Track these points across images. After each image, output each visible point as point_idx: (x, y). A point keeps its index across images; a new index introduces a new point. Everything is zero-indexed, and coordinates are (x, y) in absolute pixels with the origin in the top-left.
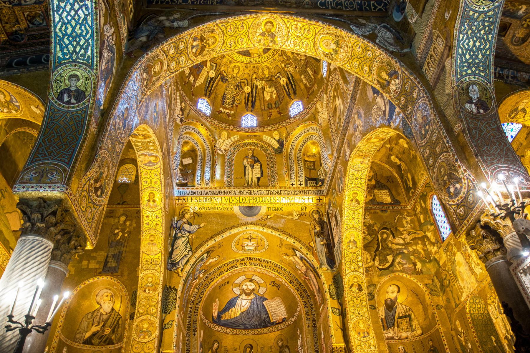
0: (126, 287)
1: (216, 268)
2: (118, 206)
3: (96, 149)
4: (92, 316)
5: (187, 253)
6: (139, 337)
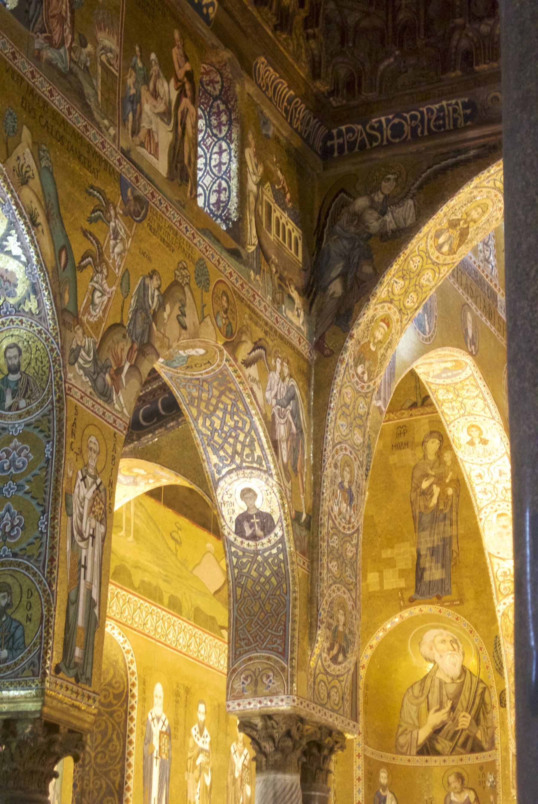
2: (414, 411)
3: (315, 599)
4: (422, 690)
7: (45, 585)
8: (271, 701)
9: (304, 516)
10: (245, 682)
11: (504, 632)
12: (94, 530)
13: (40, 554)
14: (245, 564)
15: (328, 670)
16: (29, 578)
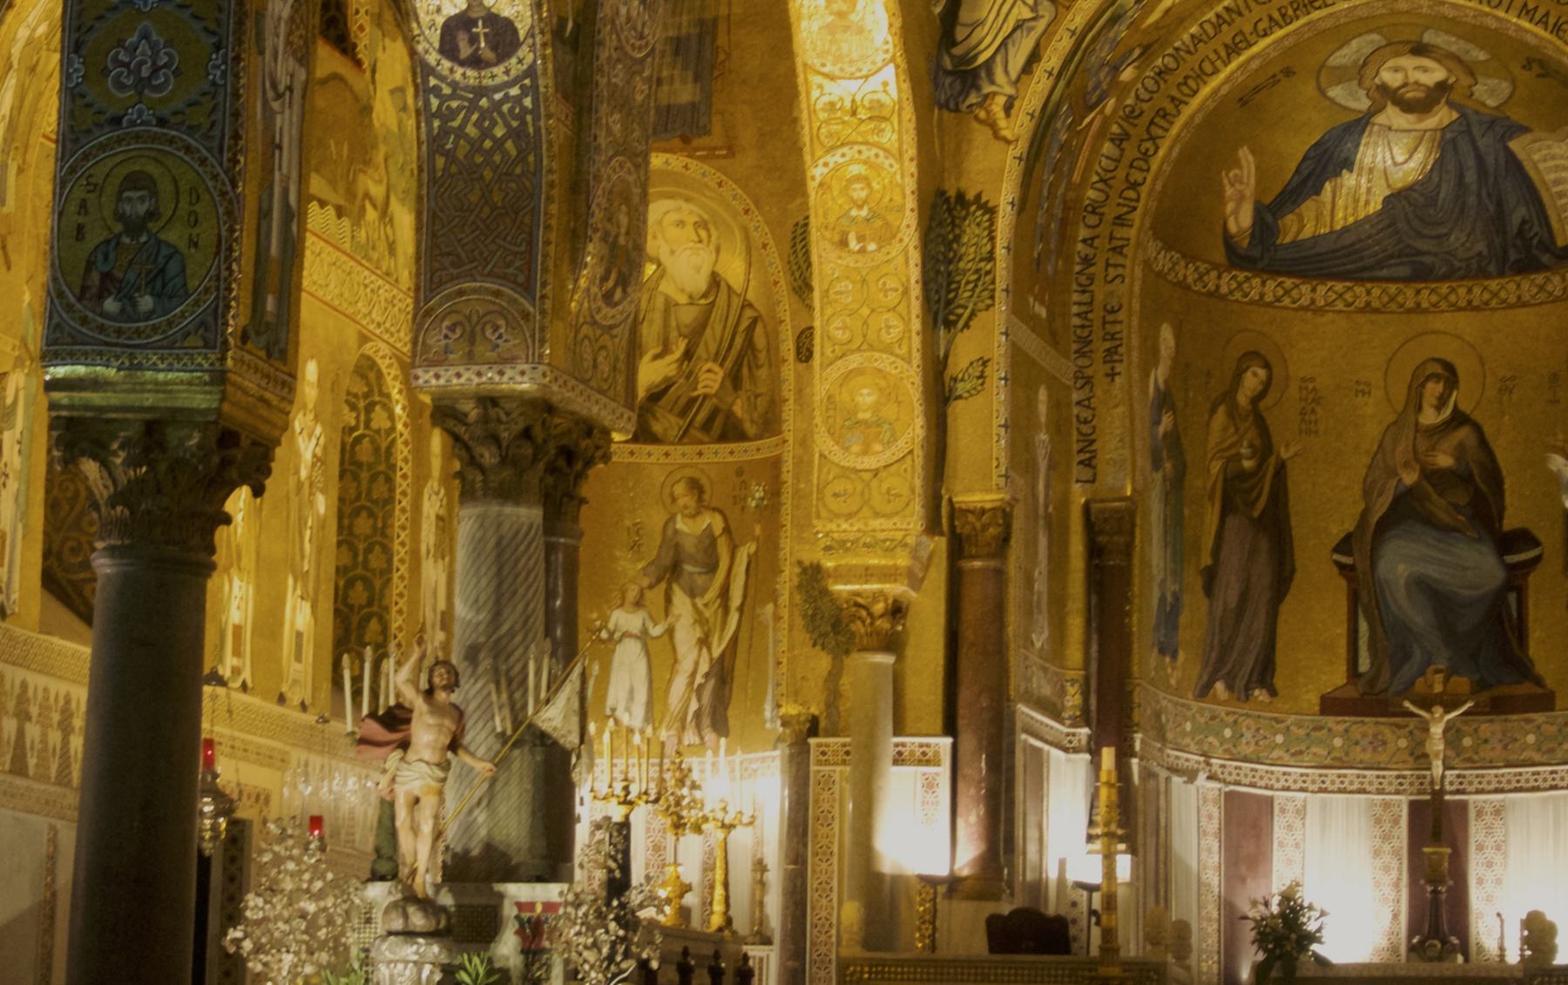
0: (757, 203)
1: (1211, 15)
5: (1027, 14)
6: (847, 449)
7: (224, 184)
8: (501, 373)
9: (570, 25)
10: (450, 334)
11: (821, 220)
12: (292, 76)
13: (213, 124)
14: (453, 114)
15: (598, 317)
16: (192, 167)
